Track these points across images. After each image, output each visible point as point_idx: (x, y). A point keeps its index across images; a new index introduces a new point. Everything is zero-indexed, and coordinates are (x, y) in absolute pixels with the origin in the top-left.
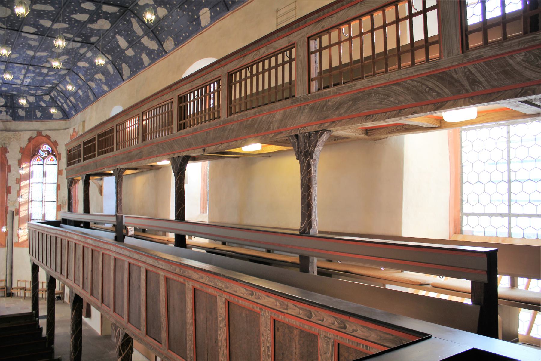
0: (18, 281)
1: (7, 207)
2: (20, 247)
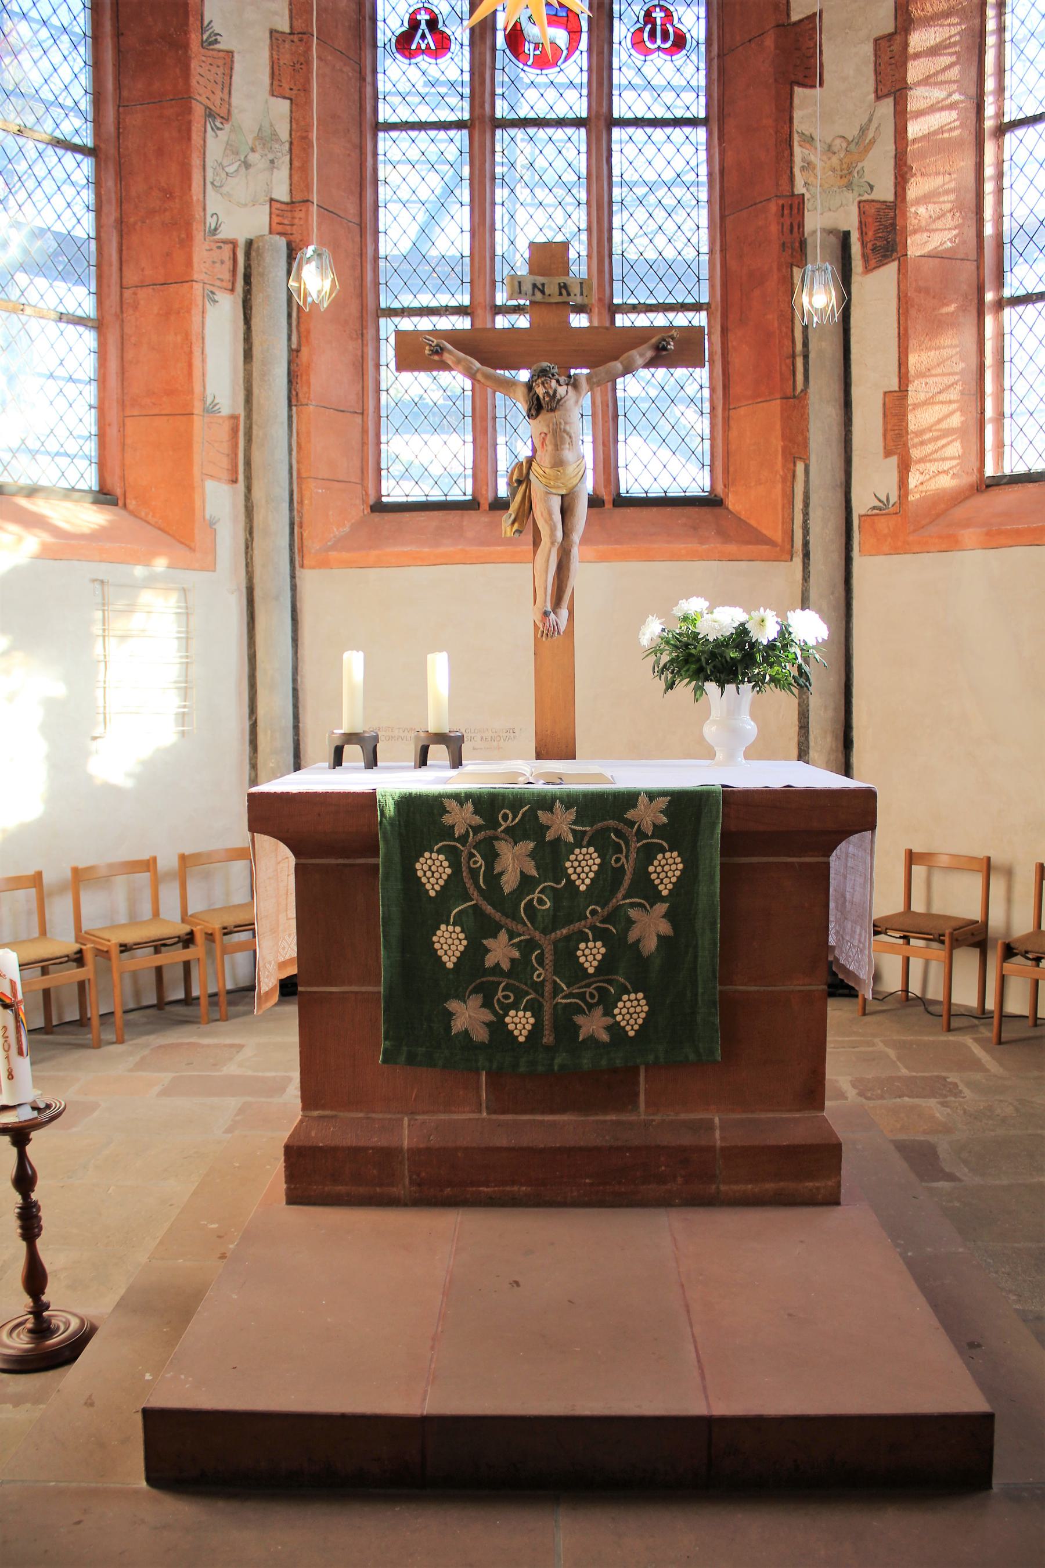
0: (911, 858)
1: (796, 206)
2: (923, 548)
